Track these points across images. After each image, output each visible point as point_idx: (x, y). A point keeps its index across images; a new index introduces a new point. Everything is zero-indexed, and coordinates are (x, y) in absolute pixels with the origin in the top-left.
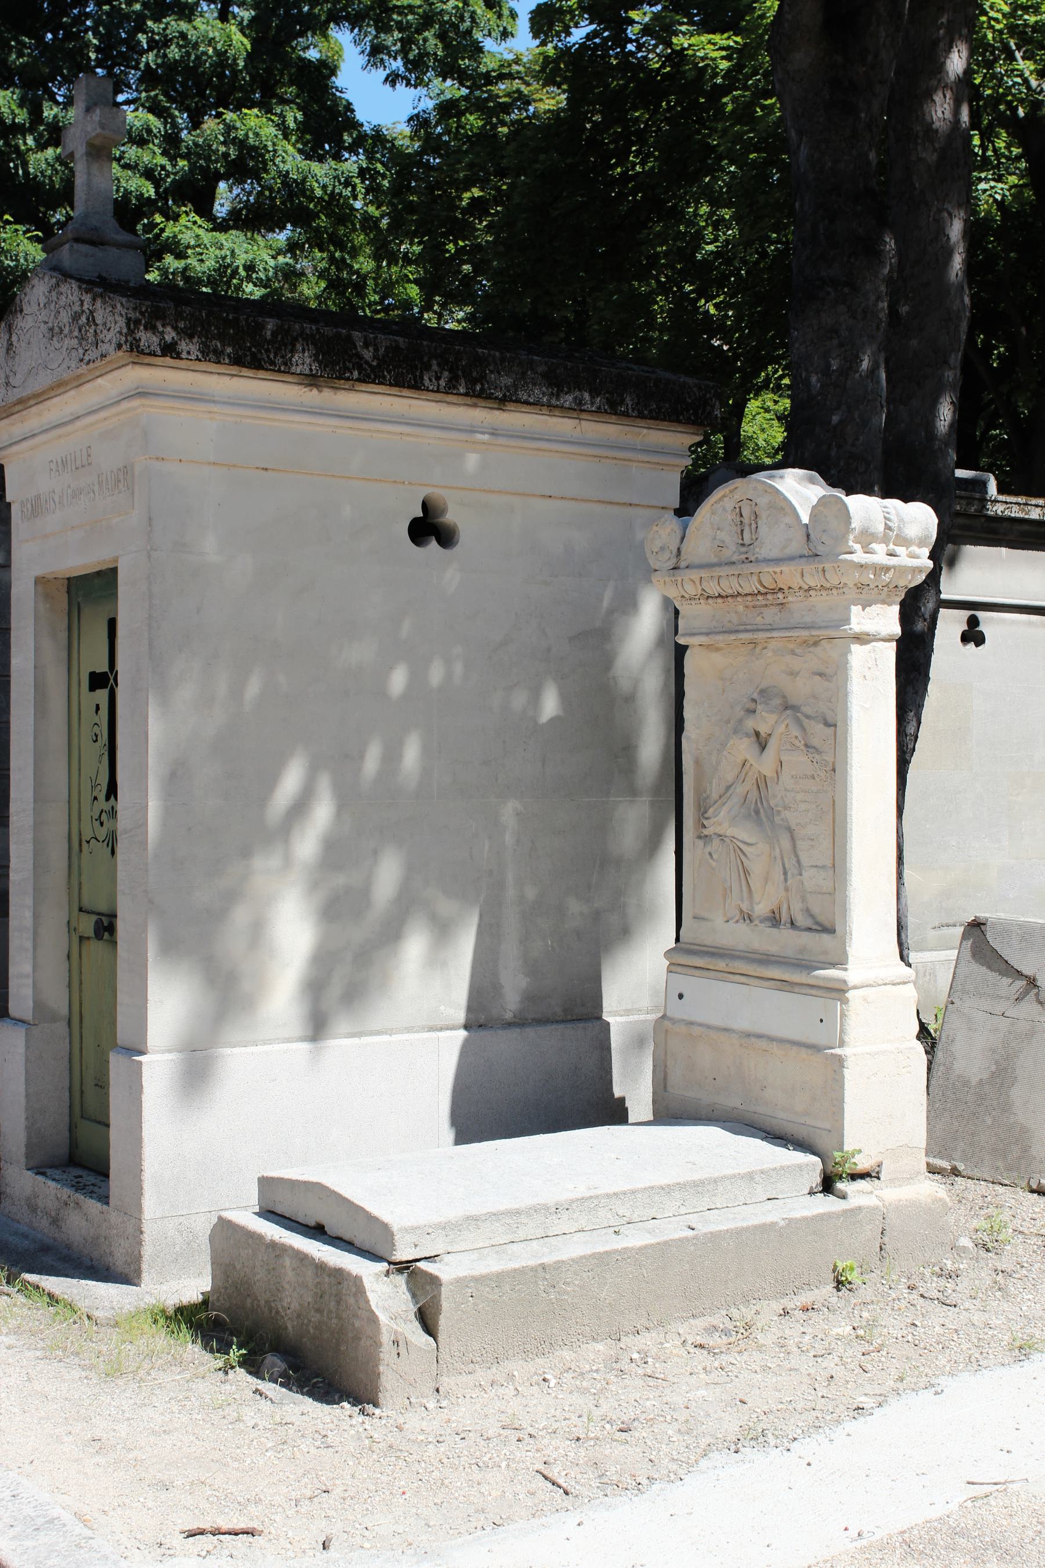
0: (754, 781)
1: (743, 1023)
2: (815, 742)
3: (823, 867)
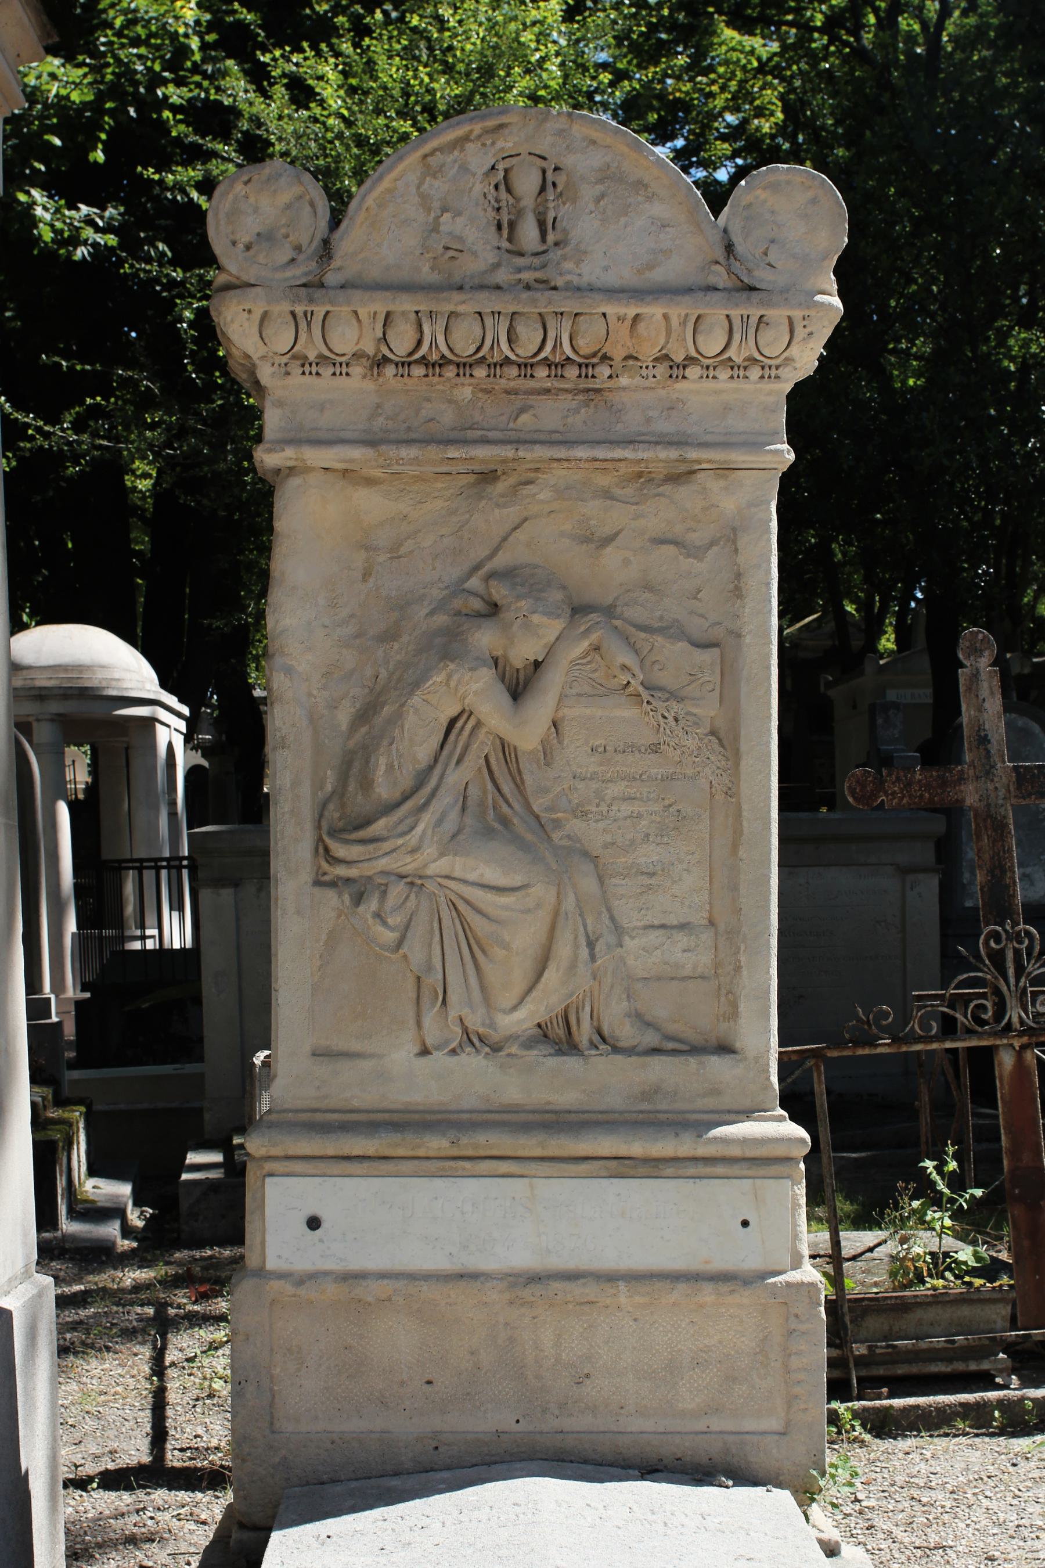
0: (482, 761)
1: (518, 1254)
3: (682, 927)
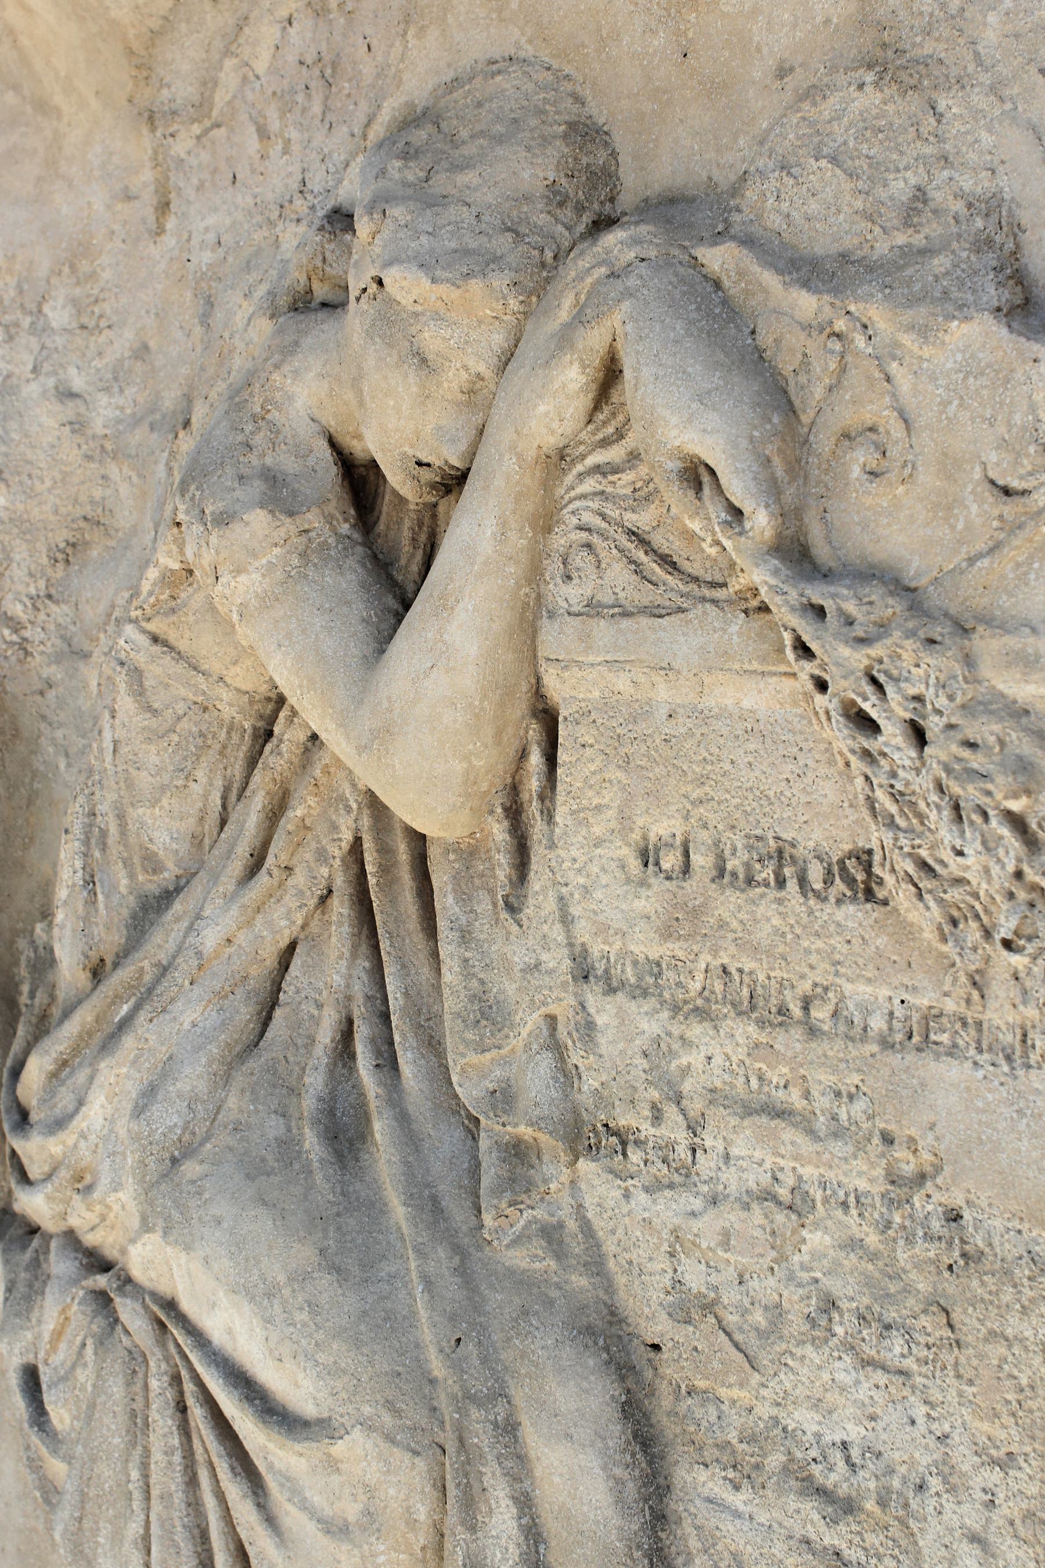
2: (890, 521)
